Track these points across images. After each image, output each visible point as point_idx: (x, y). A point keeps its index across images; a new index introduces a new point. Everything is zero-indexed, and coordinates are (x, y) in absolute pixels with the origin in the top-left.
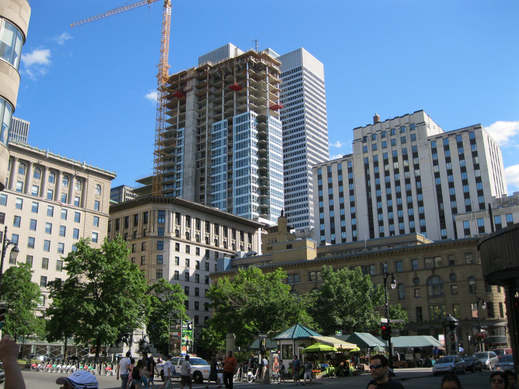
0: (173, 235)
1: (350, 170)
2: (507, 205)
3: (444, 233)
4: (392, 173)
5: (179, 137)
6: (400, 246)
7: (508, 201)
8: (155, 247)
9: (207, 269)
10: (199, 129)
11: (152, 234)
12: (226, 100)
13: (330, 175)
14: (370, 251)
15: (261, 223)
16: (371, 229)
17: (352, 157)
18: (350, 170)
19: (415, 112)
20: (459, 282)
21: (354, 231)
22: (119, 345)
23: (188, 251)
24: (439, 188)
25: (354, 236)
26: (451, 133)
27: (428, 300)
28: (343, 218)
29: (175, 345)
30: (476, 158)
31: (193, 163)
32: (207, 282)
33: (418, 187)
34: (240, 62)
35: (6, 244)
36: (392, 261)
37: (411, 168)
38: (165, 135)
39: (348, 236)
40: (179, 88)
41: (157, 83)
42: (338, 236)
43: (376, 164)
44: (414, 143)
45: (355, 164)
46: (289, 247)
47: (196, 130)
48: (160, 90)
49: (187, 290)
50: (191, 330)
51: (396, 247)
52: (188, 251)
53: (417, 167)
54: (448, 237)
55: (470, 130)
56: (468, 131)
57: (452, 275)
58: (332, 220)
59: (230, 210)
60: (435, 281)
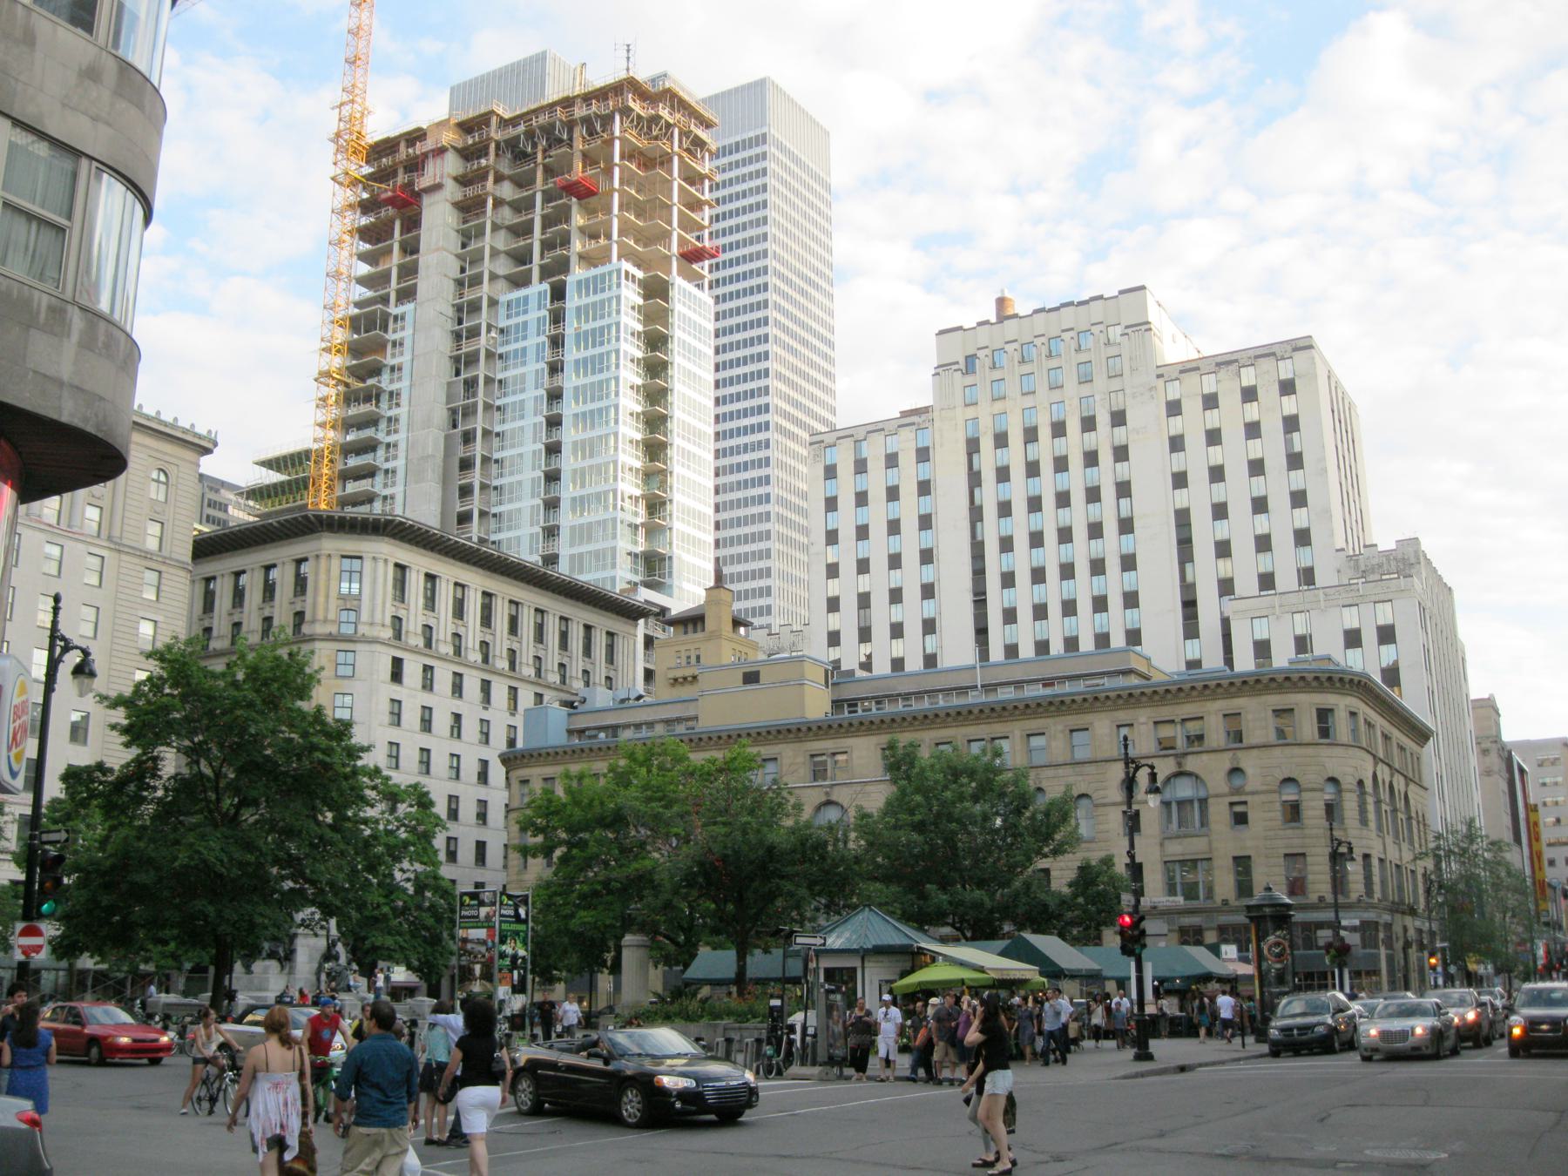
0: (387, 633)
1: (923, 455)
2: (1377, 577)
3: (1193, 649)
4: (1047, 467)
5: (395, 331)
6: (1080, 686)
7: (1380, 566)
9: (486, 737)
10: (459, 309)
11: (320, 629)
12: (548, 222)
13: (861, 467)
14: (992, 698)
15: (647, 602)
16: (982, 632)
17: (930, 415)
18: (923, 455)
19: (1121, 292)
20: (1253, 793)
21: (928, 637)
22: (258, 966)
23: (428, 685)
24: (1183, 519)
25: (929, 651)
26: (1227, 358)
27: (1162, 845)
28: (896, 596)
29: (478, 968)
30: (1296, 435)
31: (440, 415)
32: (483, 777)
33: (1124, 514)
34: (594, 108)
35: (58, 650)
36: (1060, 727)
37: (1106, 457)
38: (354, 323)
39: (911, 650)
40: (401, 178)
41: (331, 158)
42: (883, 650)
43: (1001, 440)
44: (1115, 384)
45: (937, 436)
46: (751, 678)
47: (450, 312)
48: (341, 184)
50: (525, 922)
51: (1068, 688)
52: (428, 685)
53: (1121, 453)
54: (1206, 665)
55: (1279, 354)
56: (1274, 354)
57: (1236, 771)
58: (864, 600)
59: (551, 559)
60: (1184, 789)
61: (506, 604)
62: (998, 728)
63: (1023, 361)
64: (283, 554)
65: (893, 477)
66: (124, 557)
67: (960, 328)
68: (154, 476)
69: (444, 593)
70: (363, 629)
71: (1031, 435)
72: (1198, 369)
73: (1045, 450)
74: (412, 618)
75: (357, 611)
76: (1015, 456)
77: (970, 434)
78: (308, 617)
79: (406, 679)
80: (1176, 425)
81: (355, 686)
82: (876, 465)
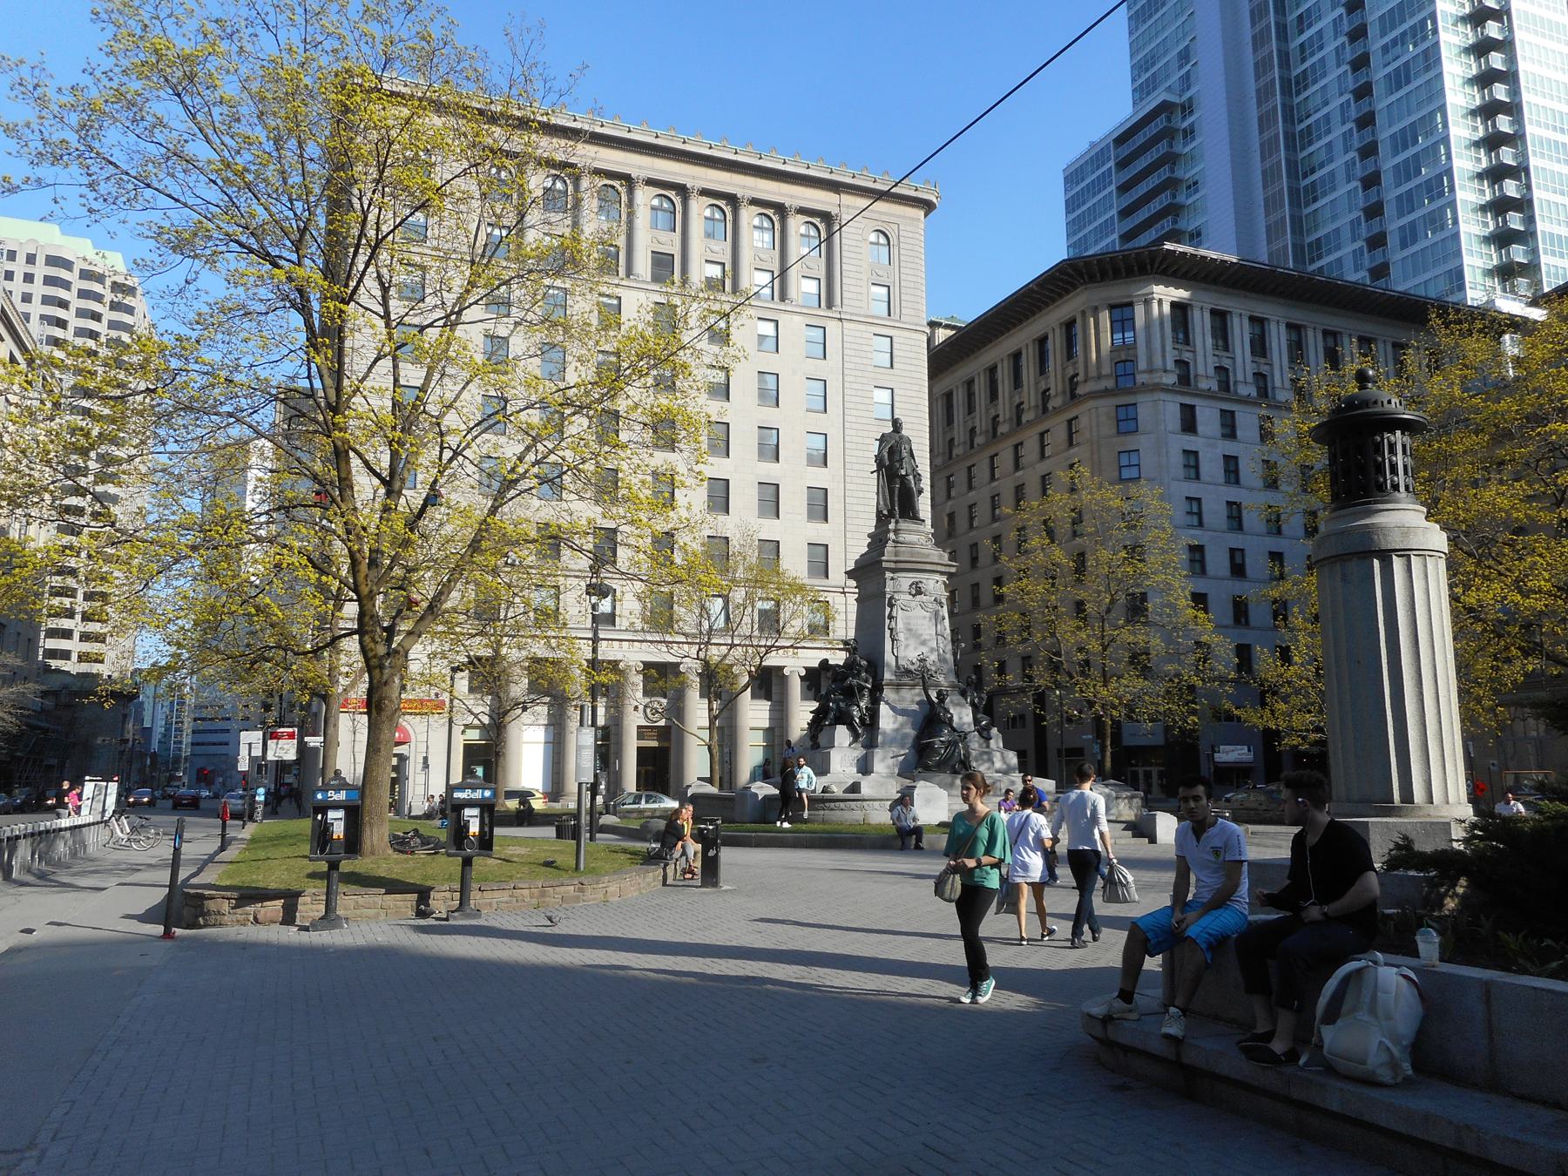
0: (1170, 379)
8: (1108, 428)
32: (1311, 531)
49: (1238, 560)
64: (1049, 321)
69: (1237, 330)
70: (1141, 378)
74: (1200, 359)
75: (1133, 361)
79: (1200, 428)
81: (1142, 442)
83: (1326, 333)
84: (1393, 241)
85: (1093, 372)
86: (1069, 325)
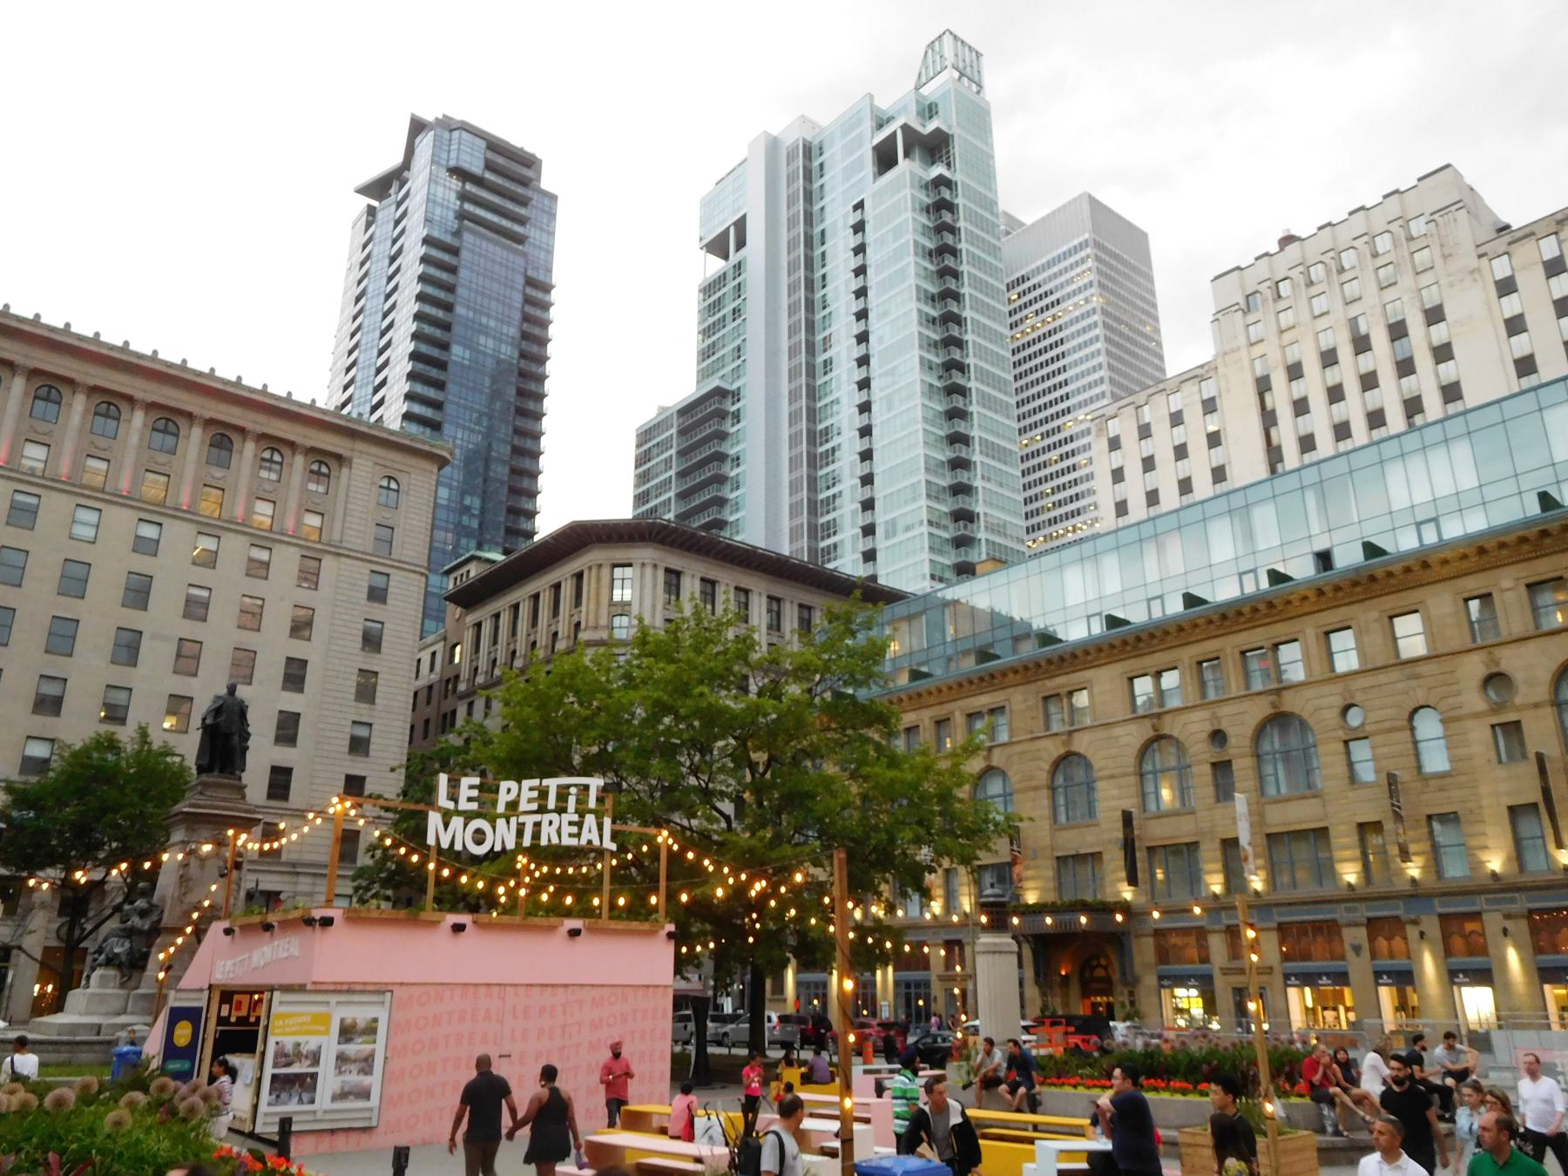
1: (1209, 406)
13: (1145, 432)
18: (1209, 406)
43: (1295, 372)
44: (1427, 279)
53: (1443, 353)
59: (874, 578)
61: (796, 609)
62: (1280, 630)
63: (1310, 283)
64: (563, 573)
65: (1179, 435)
66: (343, 559)
67: (1238, 268)
68: (385, 483)
71: (1329, 359)
72: (1533, 234)
73: (1347, 372)
76: (1313, 385)
77: (1259, 372)
78: (583, 625)
80: (1511, 306)
82: (1161, 429)
83: (801, 606)
84: (880, 531)
85: (591, 623)
86: (579, 576)
